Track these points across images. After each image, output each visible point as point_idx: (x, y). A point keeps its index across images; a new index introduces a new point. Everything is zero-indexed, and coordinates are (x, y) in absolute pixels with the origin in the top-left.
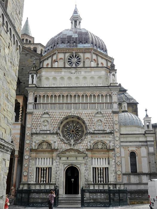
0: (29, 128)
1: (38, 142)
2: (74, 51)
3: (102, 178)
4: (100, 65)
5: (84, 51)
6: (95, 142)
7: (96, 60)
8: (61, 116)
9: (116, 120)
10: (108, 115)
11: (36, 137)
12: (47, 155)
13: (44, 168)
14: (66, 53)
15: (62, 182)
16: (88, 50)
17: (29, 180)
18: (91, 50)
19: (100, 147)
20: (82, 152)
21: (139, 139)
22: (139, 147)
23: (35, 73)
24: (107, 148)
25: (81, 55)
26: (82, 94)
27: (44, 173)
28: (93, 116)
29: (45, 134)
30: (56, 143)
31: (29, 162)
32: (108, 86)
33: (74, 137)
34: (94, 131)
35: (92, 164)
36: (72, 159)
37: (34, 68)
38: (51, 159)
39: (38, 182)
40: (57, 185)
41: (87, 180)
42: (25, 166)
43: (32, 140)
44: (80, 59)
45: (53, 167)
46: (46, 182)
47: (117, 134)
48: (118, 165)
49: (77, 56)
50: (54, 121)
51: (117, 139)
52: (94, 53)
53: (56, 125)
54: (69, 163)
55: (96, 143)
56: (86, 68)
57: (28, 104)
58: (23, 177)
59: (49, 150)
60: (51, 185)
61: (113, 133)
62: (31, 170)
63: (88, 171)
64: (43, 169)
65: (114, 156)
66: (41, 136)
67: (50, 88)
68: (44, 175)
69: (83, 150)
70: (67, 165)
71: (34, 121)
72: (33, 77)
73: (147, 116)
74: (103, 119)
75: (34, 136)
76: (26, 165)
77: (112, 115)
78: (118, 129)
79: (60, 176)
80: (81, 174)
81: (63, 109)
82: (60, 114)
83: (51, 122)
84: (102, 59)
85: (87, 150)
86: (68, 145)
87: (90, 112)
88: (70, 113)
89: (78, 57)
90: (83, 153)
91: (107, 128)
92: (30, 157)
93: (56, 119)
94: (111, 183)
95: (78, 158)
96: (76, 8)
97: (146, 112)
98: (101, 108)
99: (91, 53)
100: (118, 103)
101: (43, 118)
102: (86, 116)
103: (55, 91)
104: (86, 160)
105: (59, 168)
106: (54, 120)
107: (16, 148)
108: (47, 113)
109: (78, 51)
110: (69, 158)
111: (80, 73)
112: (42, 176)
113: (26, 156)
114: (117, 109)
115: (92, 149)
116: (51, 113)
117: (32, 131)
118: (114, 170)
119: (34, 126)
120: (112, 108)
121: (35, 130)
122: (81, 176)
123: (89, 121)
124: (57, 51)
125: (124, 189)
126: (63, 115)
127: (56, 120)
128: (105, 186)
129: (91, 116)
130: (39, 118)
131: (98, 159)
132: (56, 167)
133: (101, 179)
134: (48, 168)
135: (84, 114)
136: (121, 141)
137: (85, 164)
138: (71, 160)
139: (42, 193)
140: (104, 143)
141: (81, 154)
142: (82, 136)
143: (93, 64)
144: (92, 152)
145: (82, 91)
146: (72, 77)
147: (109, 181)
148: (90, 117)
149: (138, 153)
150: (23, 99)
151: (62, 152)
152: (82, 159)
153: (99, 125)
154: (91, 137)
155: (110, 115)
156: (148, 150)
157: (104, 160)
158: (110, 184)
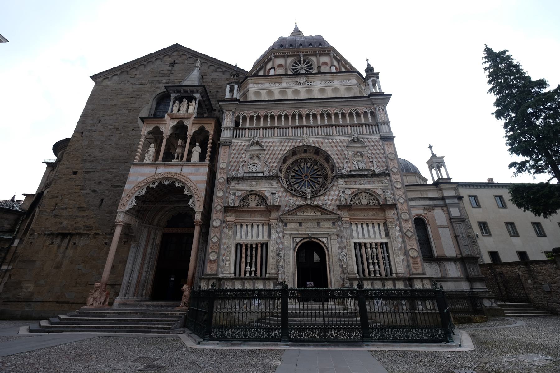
0: (223, 169)
1: (241, 194)
2: (301, 52)
3: (376, 264)
5: (317, 52)
6: (354, 192)
7: (338, 67)
8: (284, 148)
9: (390, 151)
10: (373, 144)
11: (237, 185)
12: (258, 218)
13: (251, 245)
14: (288, 56)
16: (325, 51)
17: (220, 270)
18: (330, 51)
19: (364, 201)
21: (427, 194)
22: (430, 208)
23: (236, 83)
24: (379, 203)
27: (251, 255)
28: (344, 146)
29: (255, 179)
30: (276, 195)
31: (222, 232)
32: (368, 97)
34: (351, 171)
36: (309, 225)
37: (235, 76)
38: (266, 228)
40: (280, 280)
42: (213, 240)
43: (228, 191)
44: (311, 65)
45: (271, 243)
47: (397, 176)
48: (410, 238)
49: (307, 61)
50: (272, 156)
53: (274, 162)
54: (304, 234)
55: (356, 195)
56: (323, 75)
57: (223, 129)
58: (208, 264)
59: (262, 208)
60: (267, 282)
61: (388, 175)
62: (224, 249)
64: (251, 248)
65: (398, 219)
66: (246, 182)
67: (263, 103)
68: (251, 259)
69: (331, 207)
70: (299, 239)
73: (434, 156)
76: (215, 240)
77: (381, 143)
78: (397, 167)
79: (286, 261)
80: (331, 258)
82: (282, 144)
86: (299, 199)
87: (338, 140)
88: (300, 142)
90: (332, 213)
91: (375, 166)
92: (224, 222)
93: (274, 152)
94: (400, 275)
95: (321, 224)
97: (432, 151)
99: (330, 56)
102: (332, 147)
104: (339, 228)
105: (283, 244)
106: (270, 154)
107: (197, 208)
108: (258, 144)
109: (309, 52)
110: (303, 224)
111: (313, 83)
112: (249, 261)
113: (216, 220)
115: (351, 205)
116: (266, 142)
118: (401, 248)
119: (232, 166)
122: (331, 260)
123: (337, 154)
124: (273, 54)
126: (287, 146)
127: (275, 154)
128: (386, 282)
129: (340, 146)
130: (242, 152)
131: (362, 227)
132: (277, 243)
133: (374, 268)
134: (259, 245)
135: (326, 143)
137: (338, 236)
140: (372, 195)
141: (330, 216)
144: (350, 212)
145: (320, 107)
146: (300, 89)
147: (394, 271)
148: (339, 148)
149: (430, 221)
150: (215, 126)
151: (288, 211)
152: (331, 227)
153: (357, 160)
154: (345, 183)
155: (376, 143)
156: (449, 213)
157: (376, 227)
158: (399, 279)
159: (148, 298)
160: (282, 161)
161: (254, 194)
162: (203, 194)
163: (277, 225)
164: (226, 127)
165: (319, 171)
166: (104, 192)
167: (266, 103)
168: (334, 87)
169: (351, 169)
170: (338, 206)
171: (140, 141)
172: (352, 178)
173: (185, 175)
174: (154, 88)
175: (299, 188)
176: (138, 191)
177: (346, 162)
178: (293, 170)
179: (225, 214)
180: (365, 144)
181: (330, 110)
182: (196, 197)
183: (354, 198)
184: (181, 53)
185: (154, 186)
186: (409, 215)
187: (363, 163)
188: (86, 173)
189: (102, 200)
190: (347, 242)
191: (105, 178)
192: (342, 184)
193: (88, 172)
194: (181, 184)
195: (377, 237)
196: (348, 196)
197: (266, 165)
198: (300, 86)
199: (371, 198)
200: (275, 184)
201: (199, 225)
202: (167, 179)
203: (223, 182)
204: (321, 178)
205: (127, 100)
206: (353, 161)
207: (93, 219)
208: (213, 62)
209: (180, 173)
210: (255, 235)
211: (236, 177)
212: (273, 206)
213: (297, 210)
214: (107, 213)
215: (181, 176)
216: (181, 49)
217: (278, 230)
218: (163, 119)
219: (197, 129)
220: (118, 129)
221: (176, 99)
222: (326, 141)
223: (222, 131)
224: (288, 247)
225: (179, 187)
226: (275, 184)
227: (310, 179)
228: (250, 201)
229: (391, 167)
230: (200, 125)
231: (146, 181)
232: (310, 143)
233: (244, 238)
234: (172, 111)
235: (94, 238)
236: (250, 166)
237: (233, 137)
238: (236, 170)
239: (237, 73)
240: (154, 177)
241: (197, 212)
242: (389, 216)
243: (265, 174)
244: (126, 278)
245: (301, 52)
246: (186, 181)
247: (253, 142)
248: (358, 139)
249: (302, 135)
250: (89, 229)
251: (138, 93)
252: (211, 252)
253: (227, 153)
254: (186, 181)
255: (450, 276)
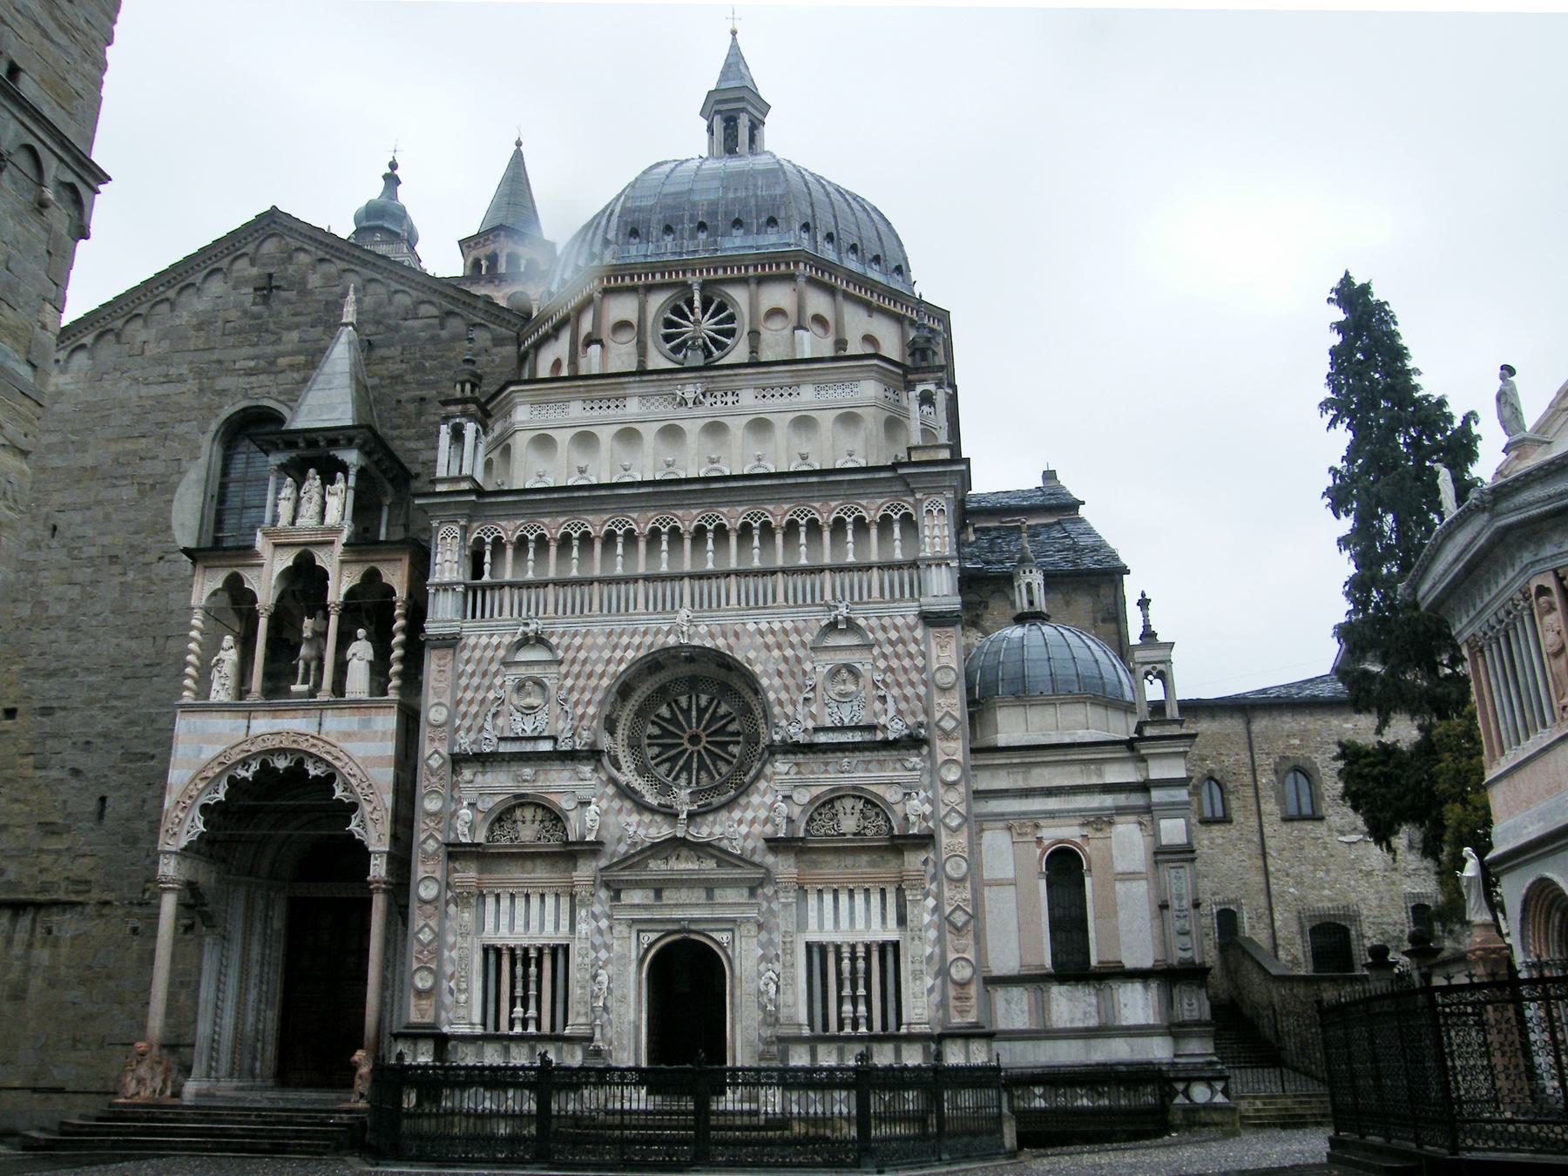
0: (439, 726)
1: (491, 805)
2: (694, 273)
4: (855, 347)
5: (751, 270)
6: (817, 798)
8: (618, 654)
9: (944, 661)
10: (894, 635)
11: (479, 778)
12: (541, 873)
13: (526, 950)
14: (650, 288)
15: (627, 1028)
16: (778, 266)
17: (443, 1015)
18: (796, 264)
19: (849, 824)
20: (739, 858)
24: (892, 828)
25: (739, 295)
26: (741, 521)
28: (803, 644)
30: (593, 807)
33: (703, 775)
34: (816, 730)
35: (802, 925)
36: (684, 895)
37: (468, 386)
38: (565, 903)
39: (497, 1027)
41: (771, 1019)
42: (421, 936)
43: (456, 796)
46: (539, 1027)
47: (953, 744)
50: (581, 682)
51: (952, 777)
52: (811, 281)
53: (589, 702)
55: (828, 803)
57: (432, 591)
59: (554, 844)
60: (565, 1047)
62: (453, 961)
63: (778, 967)
64: (523, 957)
65: (934, 878)
66: (505, 768)
68: (526, 987)
69: (750, 844)
71: (466, 688)
72: (458, 435)
74: (863, 662)
75: (467, 774)
77: (919, 633)
78: (957, 714)
80: (737, 985)
81: (631, 610)
82: (615, 639)
83: (560, 688)
84: (870, 316)
85: (775, 845)
86: (658, 818)
87: (788, 625)
88: (669, 633)
89: (722, 308)
91: (892, 712)
93: (588, 668)
95: (717, 892)
96: (735, 49)
98: (856, 598)
100: (954, 564)
101: (513, 670)
102: (768, 647)
103: (586, 512)
104: (765, 904)
105: (608, 948)
106: (578, 676)
108: (540, 640)
109: (720, 272)
110: (666, 894)
111: (730, 399)
112: (519, 992)
113: (427, 882)
114: (945, 600)
116: (563, 634)
117: (453, 743)
118: (930, 957)
119: (465, 715)
120: (917, 589)
121: (473, 735)
122: (738, 993)
123: (780, 674)
125: (990, 1061)
126: (627, 647)
127: (590, 675)
129: (792, 646)
130: (494, 667)
131: (836, 899)
132: (594, 947)
134: (546, 951)
135: (751, 635)
136: (977, 792)
137: (760, 926)
138: (676, 905)
139: (518, 1086)
140: (871, 803)
142: (745, 769)
143: (810, 344)
144: (806, 857)
145: (740, 503)
148: (789, 652)
150: (412, 564)
152: (742, 900)
153: (840, 695)
154: (794, 770)
155: (906, 634)
157: (875, 899)
159: (270, 1082)
160: (611, 699)
161: (530, 804)
162: (388, 799)
163: (592, 895)
164: (440, 585)
165: (734, 719)
166: (106, 776)
167: (565, 495)
168: (799, 414)
169: (820, 723)
170: (767, 840)
171: (193, 628)
172: (814, 753)
173: (334, 741)
174: (209, 395)
175: (670, 779)
176: (207, 792)
177: (805, 699)
178: (653, 718)
179: (451, 865)
180: (871, 636)
181: (771, 513)
182: (368, 808)
183: (820, 814)
184: (294, 244)
185: (249, 775)
186: (968, 865)
187: (855, 703)
188: (43, 715)
189: (103, 799)
190: (784, 943)
191: (99, 728)
192: (787, 773)
193: (47, 711)
194: (324, 768)
195: (873, 927)
196: (801, 808)
197: (563, 715)
198: (683, 411)
199: (868, 813)
200: (589, 775)
201: (384, 890)
202: (282, 752)
203: (441, 766)
204: (738, 743)
205: (129, 446)
206: (826, 697)
207: (86, 860)
208: (402, 277)
209: (316, 734)
210: (534, 923)
211: (475, 754)
212: (582, 842)
213: (649, 853)
214: (125, 841)
215: (320, 744)
216: (291, 229)
217: (597, 909)
218: (251, 552)
219: (357, 581)
220: (114, 559)
221: (284, 469)
222: (751, 627)
223: (431, 598)
224: (622, 957)
225: (316, 777)
226: (589, 775)
227: (705, 748)
228: (519, 823)
229: (938, 716)
230: (366, 567)
231: (222, 759)
232: (701, 637)
233: (504, 930)
234: (275, 518)
235: (101, 916)
236: (518, 716)
237: (465, 617)
238: (475, 728)
239: (474, 374)
240: (245, 747)
241: (375, 852)
242: (910, 868)
243: (560, 740)
244: (204, 1028)
245: (694, 273)
246: (337, 758)
247: (525, 634)
248: (848, 620)
249: (677, 607)
250: (83, 887)
251: (161, 417)
252: (418, 969)
253: (449, 674)
254: (337, 758)
255: (1124, 1023)
